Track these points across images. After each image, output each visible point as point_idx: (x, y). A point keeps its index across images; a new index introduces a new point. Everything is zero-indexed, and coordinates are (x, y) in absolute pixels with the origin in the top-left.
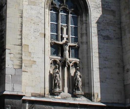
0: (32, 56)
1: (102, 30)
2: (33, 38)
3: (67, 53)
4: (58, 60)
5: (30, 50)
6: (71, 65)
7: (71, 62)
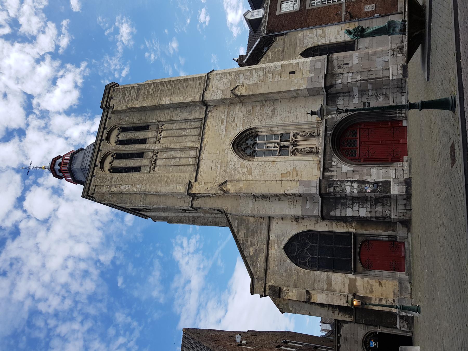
0: (289, 171)
2: (276, 170)
3: (286, 144)
5: (285, 173)
6: (295, 140)
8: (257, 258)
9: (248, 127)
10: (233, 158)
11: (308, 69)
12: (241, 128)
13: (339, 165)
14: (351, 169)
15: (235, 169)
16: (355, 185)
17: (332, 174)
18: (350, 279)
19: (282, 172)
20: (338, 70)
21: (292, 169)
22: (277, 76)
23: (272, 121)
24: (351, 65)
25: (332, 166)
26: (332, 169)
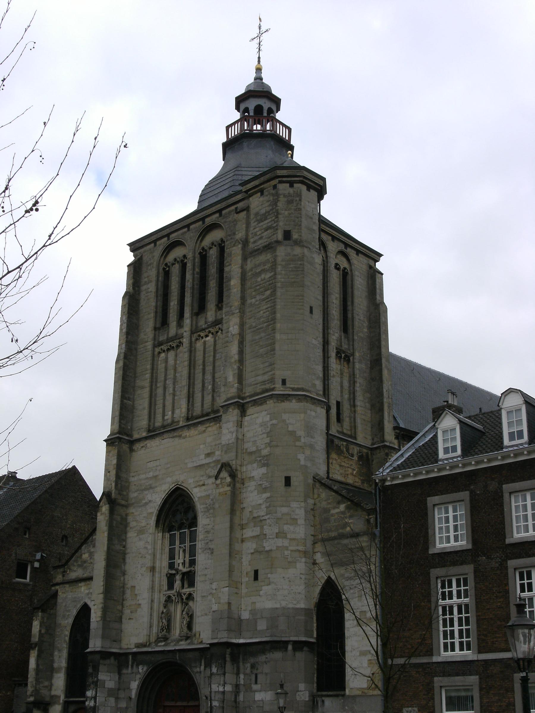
1: (211, 541)
2: (140, 575)
4: (171, 595)
5: (136, 592)
6: (184, 597)
7: (185, 594)
8: (79, 566)
9: (200, 507)
10: (156, 498)
11: (259, 606)
12: (199, 495)
13: (138, 676)
14: (133, 694)
15: (146, 504)
16: (92, 704)
17: (130, 666)
18: (59, 697)
19: (137, 588)
20: (248, 665)
21: (140, 602)
22: (254, 546)
23: (203, 551)
24: (255, 687)
25: (138, 666)
26: (135, 666)
